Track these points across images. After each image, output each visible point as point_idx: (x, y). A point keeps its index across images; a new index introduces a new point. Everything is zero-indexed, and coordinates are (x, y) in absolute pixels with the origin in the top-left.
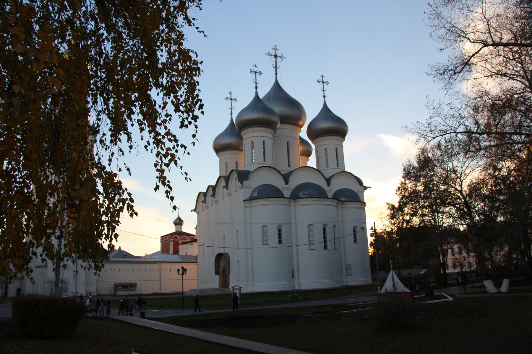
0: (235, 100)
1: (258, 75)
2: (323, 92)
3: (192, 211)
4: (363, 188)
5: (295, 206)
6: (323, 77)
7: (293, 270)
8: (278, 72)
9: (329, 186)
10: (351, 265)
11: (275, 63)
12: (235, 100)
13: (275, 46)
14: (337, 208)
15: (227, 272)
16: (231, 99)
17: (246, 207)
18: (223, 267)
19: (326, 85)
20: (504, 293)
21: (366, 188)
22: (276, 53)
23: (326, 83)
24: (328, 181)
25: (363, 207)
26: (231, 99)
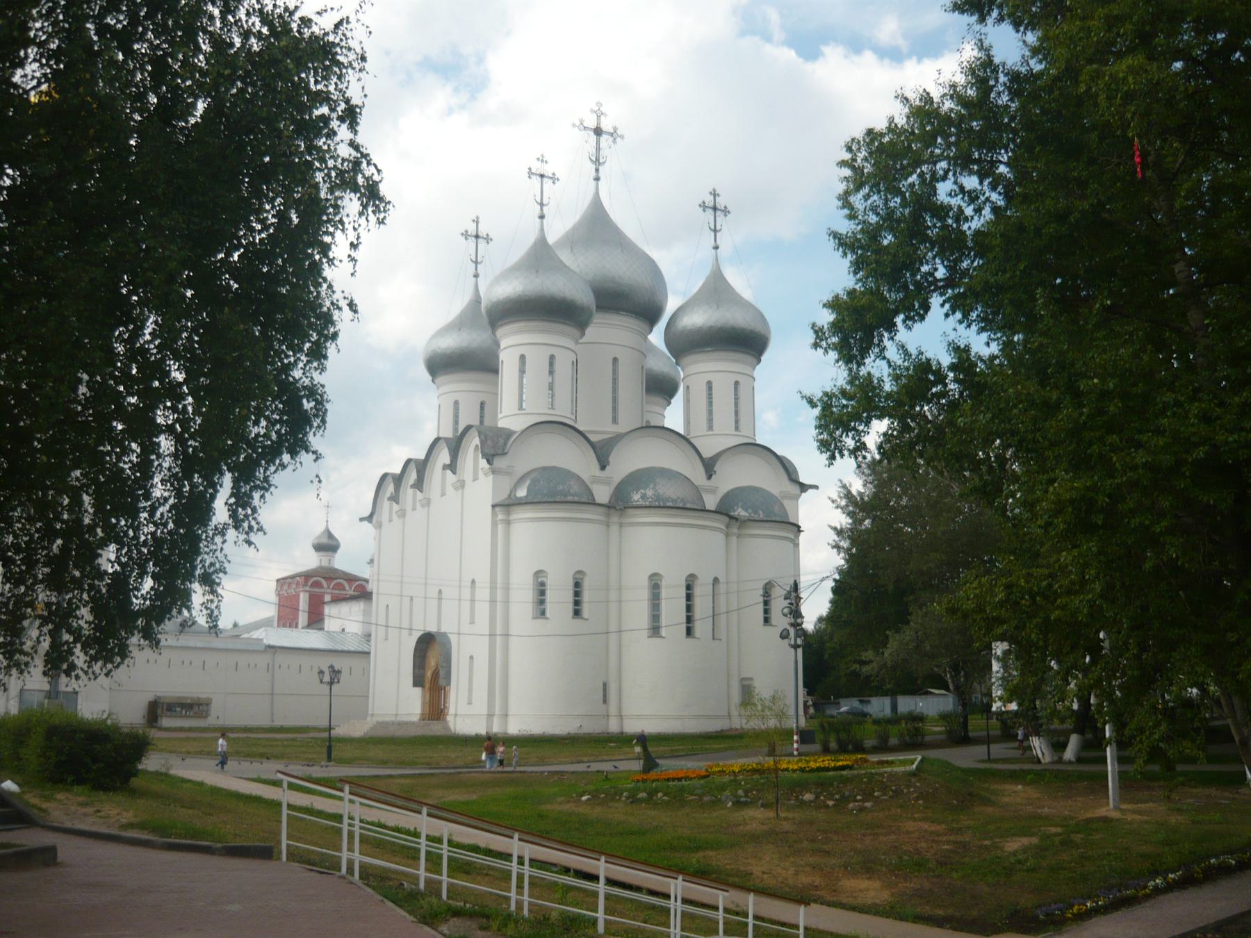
1: (548, 183)
2: (713, 234)
3: (361, 519)
4: (796, 489)
5: (621, 525)
6: (715, 194)
7: (605, 685)
8: (601, 174)
9: (709, 477)
10: (751, 679)
11: (594, 151)
13: (599, 104)
14: (727, 535)
15: (442, 682)
16: (477, 237)
17: (494, 524)
18: (433, 669)
19: (722, 216)
20: (1070, 762)
21: (804, 488)
22: (599, 123)
23: (723, 211)
24: (709, 466)
25: (793, 537)
26: (477, 237)
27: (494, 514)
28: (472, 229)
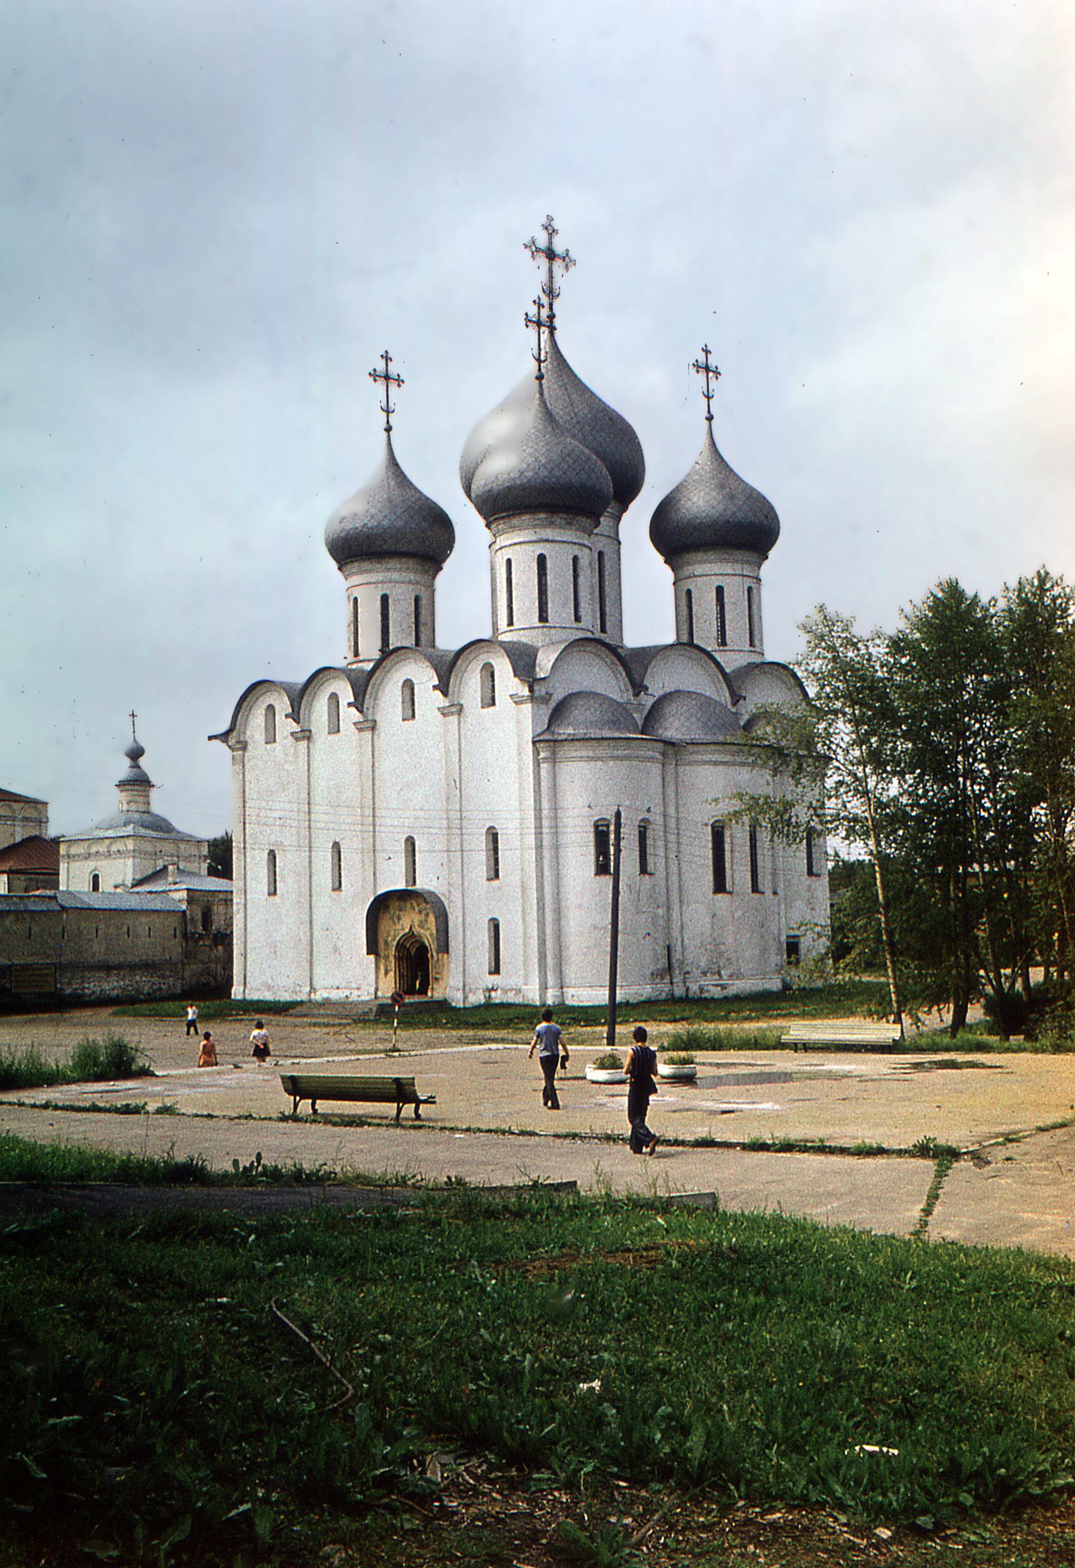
0: (399, 381)
12: (399, 381)
22: (550, 243)
26: (387, 378)
27: (536, 752)
28: (380, 366)
